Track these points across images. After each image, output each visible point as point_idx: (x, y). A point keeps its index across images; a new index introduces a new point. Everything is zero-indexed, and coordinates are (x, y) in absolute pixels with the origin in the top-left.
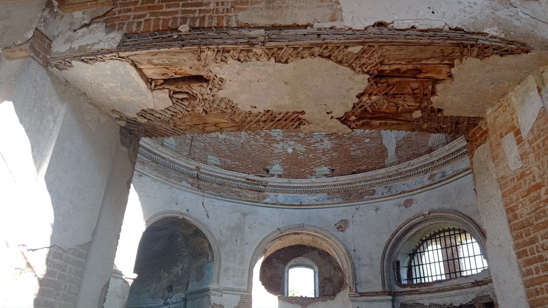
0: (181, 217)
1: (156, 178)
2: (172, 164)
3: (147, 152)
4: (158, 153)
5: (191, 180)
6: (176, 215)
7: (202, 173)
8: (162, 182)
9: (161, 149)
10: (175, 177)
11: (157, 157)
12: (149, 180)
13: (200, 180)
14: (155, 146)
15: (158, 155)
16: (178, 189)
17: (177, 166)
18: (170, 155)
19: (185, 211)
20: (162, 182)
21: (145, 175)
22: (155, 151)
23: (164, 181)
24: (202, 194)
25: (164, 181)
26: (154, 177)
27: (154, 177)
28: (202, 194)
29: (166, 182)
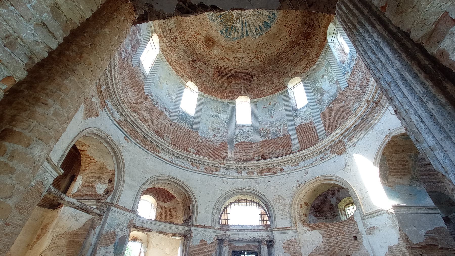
0: (389, 139)
1: (361, 136)
2: (361, 118)
3: (347, 132)
4: (349, 125)
5: (377, 109)
6: (387, 141)
7: (372, 98)
8: (366, 134)
9: (347, 123)
10: (370, 120)
11: (353, 126)
12: (359, 142)
13: (379, 101)
14: (344, 126)
15: (351, 126)
16: (376, 124)
17: (364, 115)
18: (353, 118)
19: (388, 132)
20: (366, 134)
21: (356, 142)
22: (347, 127)
23: (366, 132)
24: (385, 108)
25: (366, 132)
26: (360, 137)
27: (360, 137)
28: (385, 108)
29: (367, 130)
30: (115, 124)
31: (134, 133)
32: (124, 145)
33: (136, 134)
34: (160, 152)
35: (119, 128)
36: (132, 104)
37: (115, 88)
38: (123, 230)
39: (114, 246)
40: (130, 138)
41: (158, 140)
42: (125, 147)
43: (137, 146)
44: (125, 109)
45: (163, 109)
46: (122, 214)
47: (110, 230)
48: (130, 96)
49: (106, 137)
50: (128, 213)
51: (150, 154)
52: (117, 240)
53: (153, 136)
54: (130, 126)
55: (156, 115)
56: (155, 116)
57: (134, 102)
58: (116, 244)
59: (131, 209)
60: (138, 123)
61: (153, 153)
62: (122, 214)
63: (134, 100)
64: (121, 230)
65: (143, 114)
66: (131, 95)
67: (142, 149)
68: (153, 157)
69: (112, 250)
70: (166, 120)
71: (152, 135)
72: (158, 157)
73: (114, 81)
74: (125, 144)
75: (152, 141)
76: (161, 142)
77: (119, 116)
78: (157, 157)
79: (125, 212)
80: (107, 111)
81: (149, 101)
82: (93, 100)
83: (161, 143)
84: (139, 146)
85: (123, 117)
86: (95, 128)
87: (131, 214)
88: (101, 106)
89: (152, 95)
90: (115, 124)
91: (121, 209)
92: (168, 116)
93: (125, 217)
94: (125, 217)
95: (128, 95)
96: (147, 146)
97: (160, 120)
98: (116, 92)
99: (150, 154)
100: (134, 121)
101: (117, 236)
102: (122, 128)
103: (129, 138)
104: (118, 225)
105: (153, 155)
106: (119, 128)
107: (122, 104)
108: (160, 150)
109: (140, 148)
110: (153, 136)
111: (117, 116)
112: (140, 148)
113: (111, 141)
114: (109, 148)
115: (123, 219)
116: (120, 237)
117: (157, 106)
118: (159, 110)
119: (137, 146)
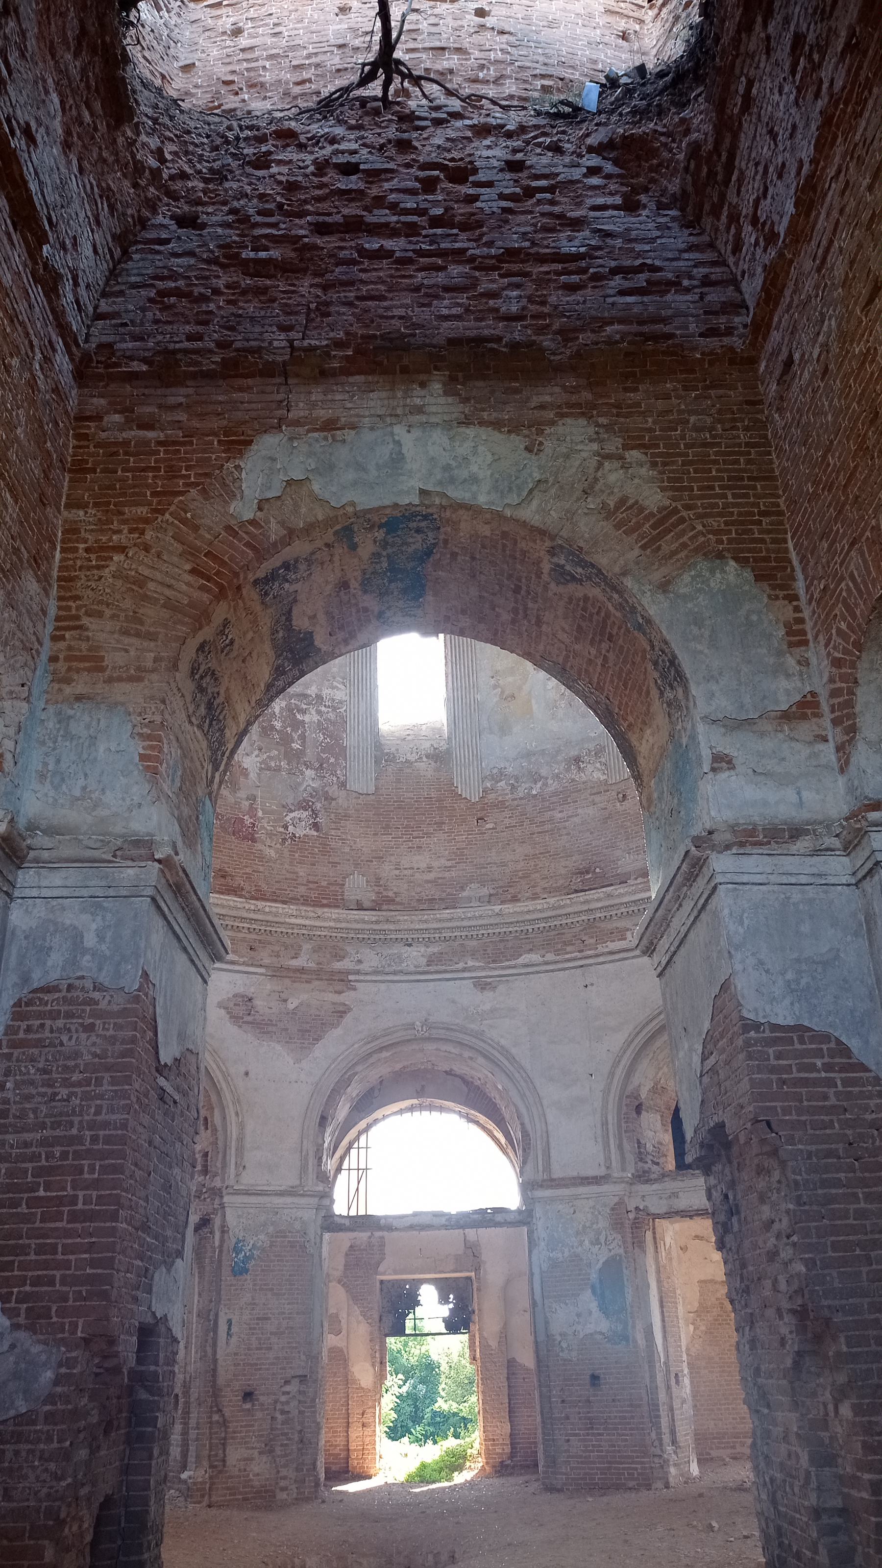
30: (418, 981)
31: (501, 946)
32: (487, 1007)
33: (510, 944)
34: (628, 930)
35: (439, 980)
36: (447, 875)
37: (332, 924)
38: (603, 1241)
39: (594, 1292)
40: (491, 974)
41: (582, 903)
42: (493, 1010)
43: (532, 973)
44: (412, 926)
45: (568, 770)
46: (576, 1197)
47: (560, 1255)
48: (423, 865)
49: (410, 1032)
50: (594, 1189)
51: (591, 965)
52: (594, 1276)
53: (563, 907)
54: (474, 943)
55: (551, 820)
56: (548, 827)
57: (449, 864)
58: (598, 1286)
59: (602, 1172)
60: (481, 916)
61: (597, 956)
62: (576, 1197)
63: (443, 862)
64: (597, 1242)
65: (503, 864)
66: (421, 861)
67: (552, 971)
68: (607, 966)
69: (594, 1306)
70: (597, 798)
71: (554, 908)
72: (622, 955)
73: (307, 922)
74: (487, 1000)
75: (569, 921)
76: (599, 900)
77: (423, 950)
78: (617, 957)
79: (582, 1190)
80: (369, 978)
81: (500, 805)
82: (291, 1006)
83: (600, 905)
84: (538, 972)
85: (429, 942)
86: (356, 1046)
87: (605, 1188)
88: (339, 986)
89: (501, 774)
90: (418, 981)
91: (566, 1186)
92: (598, 776)
93: (591, 1203)
94: (591, 1203)
95: (410, 872)
96: (569, 949)
97: (575, 819)
98: (343, 925)
99: (591, 965)
100: (465, 923)
101: (589, 1265)
102: (445, 972)
103: (491, 977)
104: (578, 1233)
105: (601, 959)
106: (439, 980)
107: (392, 927)
108: (621, 924)
109: (547, 971)
110: (563, 907)
111: (415, 955)
112: (547, 971)
113: (434, 1031)
114: (450, 1048)
115: (587, 1210)
116: (600, 1265)
117: (539, 784)
118: (555, 793)
119: (532, 973)
